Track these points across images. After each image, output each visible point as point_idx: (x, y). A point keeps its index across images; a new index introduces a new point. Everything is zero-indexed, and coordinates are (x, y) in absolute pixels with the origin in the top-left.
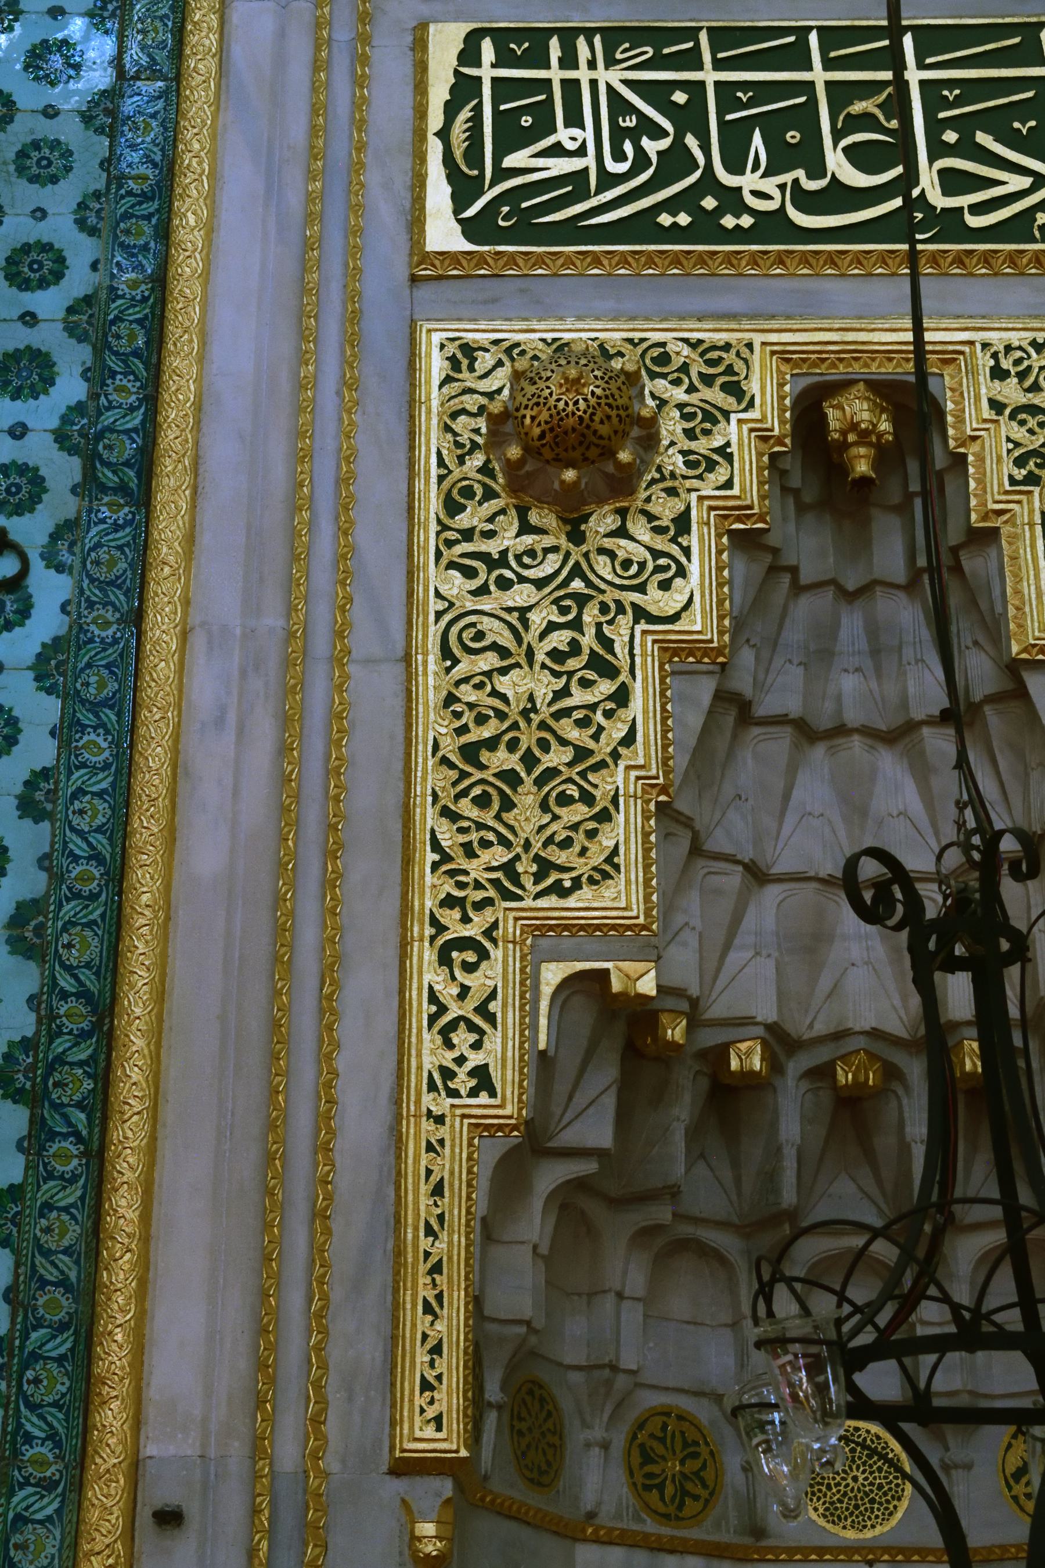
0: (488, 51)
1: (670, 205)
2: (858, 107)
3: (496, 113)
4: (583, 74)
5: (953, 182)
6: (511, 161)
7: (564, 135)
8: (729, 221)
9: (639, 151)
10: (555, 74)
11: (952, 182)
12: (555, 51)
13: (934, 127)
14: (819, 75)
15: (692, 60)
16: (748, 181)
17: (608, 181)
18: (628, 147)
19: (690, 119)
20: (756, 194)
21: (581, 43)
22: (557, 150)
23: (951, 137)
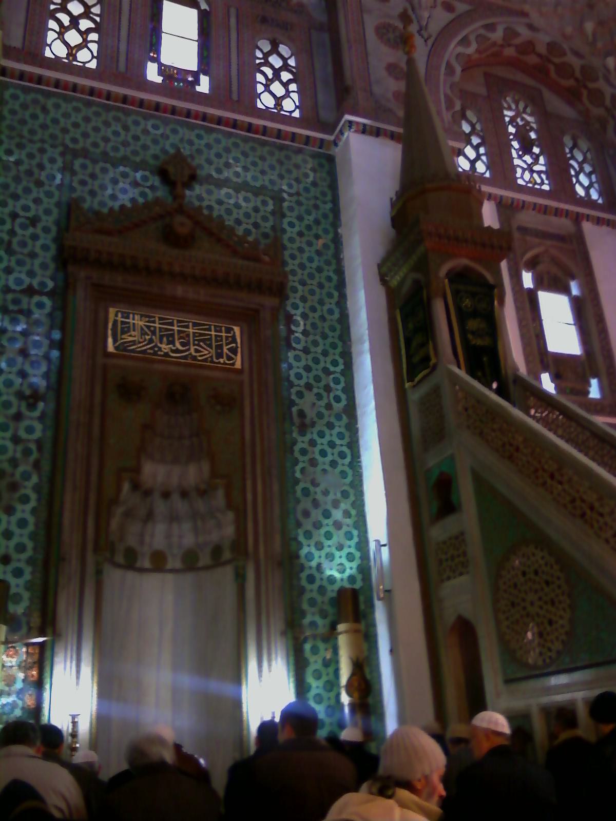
0: (120, 315)
1: (150, 349)
2: (182, 335)
4: (136, 322)
5: (197, 351)
6: (123, 336)
7: (133, 333)
8: (159, 353)
10: (131, 321)
11: (197, 351)
12: (131, 316)
13: (194, 340)
14: (176, 328)
15: (154, 322)
16: (163, 346)
17: (140, 343)
19: (154, 333)
23: (196, 342)
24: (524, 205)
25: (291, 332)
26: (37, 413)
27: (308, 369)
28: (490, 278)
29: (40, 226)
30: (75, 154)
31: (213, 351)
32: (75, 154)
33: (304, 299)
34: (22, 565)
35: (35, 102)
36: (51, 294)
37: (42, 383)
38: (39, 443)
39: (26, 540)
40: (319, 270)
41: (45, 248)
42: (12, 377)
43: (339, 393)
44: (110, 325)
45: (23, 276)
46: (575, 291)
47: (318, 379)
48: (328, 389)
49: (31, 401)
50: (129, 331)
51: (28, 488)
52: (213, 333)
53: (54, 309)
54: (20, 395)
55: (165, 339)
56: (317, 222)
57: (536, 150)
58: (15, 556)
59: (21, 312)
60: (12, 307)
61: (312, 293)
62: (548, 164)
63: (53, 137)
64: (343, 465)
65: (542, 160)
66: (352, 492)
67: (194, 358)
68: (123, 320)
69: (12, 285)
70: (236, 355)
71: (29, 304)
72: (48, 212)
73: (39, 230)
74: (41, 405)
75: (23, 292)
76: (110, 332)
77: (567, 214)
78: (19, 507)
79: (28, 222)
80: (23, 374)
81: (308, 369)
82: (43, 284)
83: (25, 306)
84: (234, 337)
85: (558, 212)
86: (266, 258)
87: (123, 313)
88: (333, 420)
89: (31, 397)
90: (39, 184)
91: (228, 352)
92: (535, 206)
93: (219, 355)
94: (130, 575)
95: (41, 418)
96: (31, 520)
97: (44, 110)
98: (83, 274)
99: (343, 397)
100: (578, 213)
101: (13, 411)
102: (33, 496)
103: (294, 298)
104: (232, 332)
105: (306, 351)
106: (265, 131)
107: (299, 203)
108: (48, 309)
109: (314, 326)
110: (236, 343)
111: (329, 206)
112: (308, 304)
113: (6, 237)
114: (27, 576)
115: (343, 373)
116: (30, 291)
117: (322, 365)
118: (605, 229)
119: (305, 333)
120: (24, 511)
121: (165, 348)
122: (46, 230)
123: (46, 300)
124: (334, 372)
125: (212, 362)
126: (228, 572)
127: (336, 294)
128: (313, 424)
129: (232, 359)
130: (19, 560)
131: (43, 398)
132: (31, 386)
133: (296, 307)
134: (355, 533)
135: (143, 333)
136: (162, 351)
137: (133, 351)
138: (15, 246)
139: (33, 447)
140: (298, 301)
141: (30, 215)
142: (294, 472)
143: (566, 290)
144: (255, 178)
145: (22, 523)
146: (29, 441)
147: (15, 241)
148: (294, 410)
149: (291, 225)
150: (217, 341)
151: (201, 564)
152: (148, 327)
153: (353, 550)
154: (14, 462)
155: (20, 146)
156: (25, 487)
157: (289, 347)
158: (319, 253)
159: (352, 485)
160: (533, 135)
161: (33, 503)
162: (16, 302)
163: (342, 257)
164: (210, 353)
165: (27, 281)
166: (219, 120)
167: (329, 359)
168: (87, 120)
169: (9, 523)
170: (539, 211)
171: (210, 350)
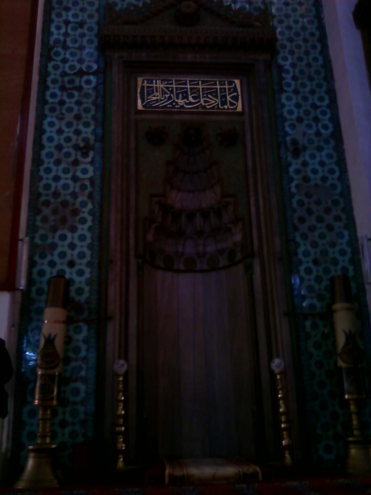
0: (146, 82)
2: (193, 91)
3: (147, 91)
4: (158, 85)
5: (205, 102)
6: (149, 97)
8: (176, 106)
9: (165, 97)
10: (154, 85)
12: (154, 82)
13: (203, 94)
14: (188, 86)
15: (172, 84)
17: (161, 100)
18: (164, 96)
20: (181, 103)
21: (158, 81)
22: (154, 96)
25: (282, 78)
26: (89, 159)
27: (298, 106)
29: (86, 27)
31: (219, 101)
33: (292, 52)
34: (83, 267)
36: (95, 74)
37: (92, 138)
38: (91, 180)
39: (85, 250)
41: (90, 42)
42: (71, 134)
43: (326, 122)
44: (139, 91)
45: (75, 63)
47: (307, 113)
48: (316, 120)
49: (85, 151)
50: (153, 92)
51: (85, 213)
52: (218, 87)
53: (98, 83)
54: (76, 147)
55: (180, 95)
58: (77, 261)
59: (75, 88)
60: (68, 86)
61: (299, 47)
64: (333, 179)
66: (341, 200)
67: (204, 107)
68: (148, 85)
70: (237, 101)
71: (80, 82)
72: (91, 16)
73: (85, 31)
74: (91, 154)
75: (75, 74)
76: (139, 95)
78: (80, 227)
79: (77, 25)
80: (78, 132)
81: (298, 106)
82: (89, 67)
83: (77, 83)
84: (235, 88)
86: (258, 24)
87: (147, 80)
88: (322, 144)
89: (84, 147)
91: (231, 100)
93: (224, 103)
94: (169, 274)
95: (92, 163)
96: (88, 235)
98: (116, 55)
99: (330, 125)
101: (72, 158)
102: (90, 218)
104: (233, 85)
105: (296, 92)
108: (94, 84)
110: (237, 92)
112: (296, 56)
113: (62, 38)
114: (87, 275)
115: (329, 106)
116: (81, 73)
117: (310, 101)
119: (294, 78)
120: (83, 229)
121: (181, 102)
123: (92, 78)
124: (320, 107)
125: (218, 108)
126: (241, 267)
127: (319, 46)
128: (305, 148)
129: (235, 104)
130: (81, 264)
131: (92, 148)
132: (86, 140)
133: (285, 59)
134: (346, 233)
135: (164, 93)
136: (178, 105)
137: (157, 107)
138: (69, 43)
139: (87, 183)
140: (287, 55)
141: (79, 20)
142: (290, 188)
145: (82, 238)
146: (84, 179)
147: (68, 40)
148: (288, 139)
150: (221, 92)
151: (221, 265)
152: (166, 88)
153: (345, 247)
154: (74, 195)
156: (83, 212)
157: (282, 91)
159: (341, 194)
161: (89, 224)
162: (71, 82)
163: (322, 16)
164: (216, 102)
165: (78, 66)
167: (316, 96)
169: (73, 238)
171: (217, 100)
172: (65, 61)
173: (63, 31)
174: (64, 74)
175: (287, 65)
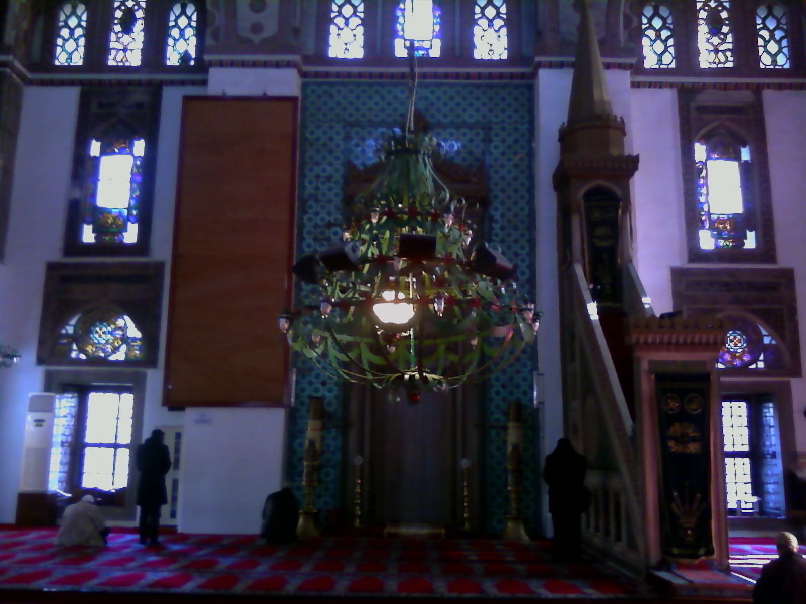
24: (704, 86)
25: (492, 228)
28: (619, 192)
30: (352, 125)
32: (352, 125)
33: (503, 203)
35: (326, 92)
40: (516, 179)
46: (745, 155)
56: (516, 141)
57: (725, 29)
60: (320, 237)
62: (736, 42)
63: (338, 115)
65: (730, 38)
69: (320, 223)
73: (333, 185)
77: (747, 86)
82: (336, 220)
85: (737, 86)
90: (331, 152)
92: (715, 86)
97: (332, 97)
99: (527, 272)
100: (758, 84)
103: (496, 204)
106: (479, 76)
107: (503, 129)
109: (509, 222)
111: (526, 126)
114: (335, 392)
115: (529, 254)
118: (787, 92)
119: (502, 228)
122: (336, 183)
133: (496, 210)
138: (320, 197)
143: (737, 157)
144: (471, 116)
149: (496, 148)
155: (319, 127)
158: (516, 166)
160: (724, 15)
166: (446, 76)
168: (358, 97)
170: (720, 89)
172: (317, 214)
173: (315, 185)
174: (316, 226)
175: (497, 215)
